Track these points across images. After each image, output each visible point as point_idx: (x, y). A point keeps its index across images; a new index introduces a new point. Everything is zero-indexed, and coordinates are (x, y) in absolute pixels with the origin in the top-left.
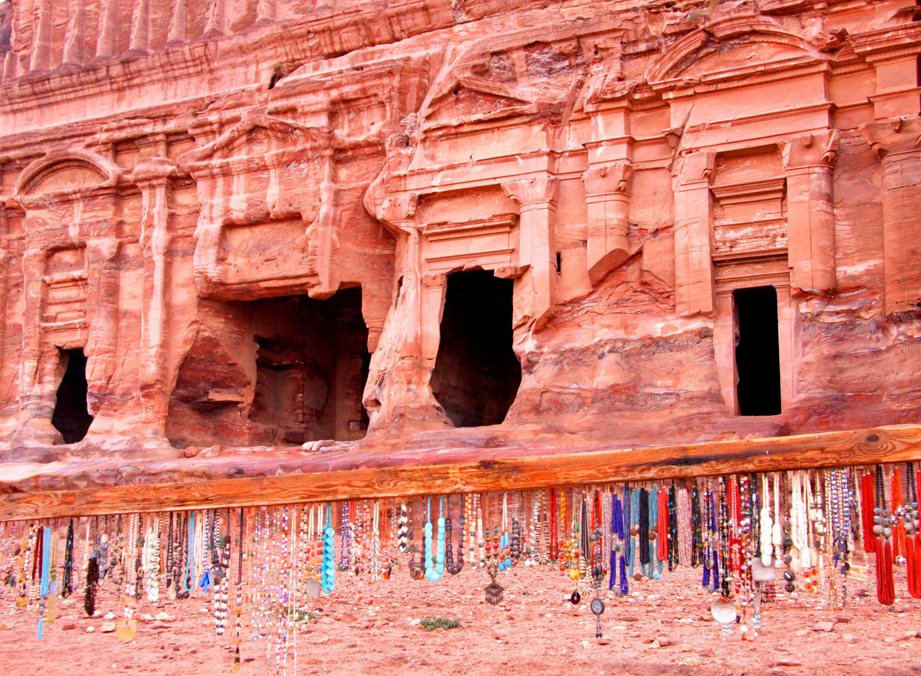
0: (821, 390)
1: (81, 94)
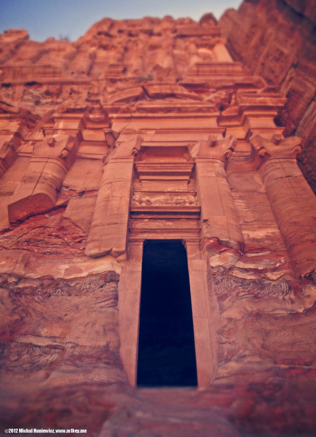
0: (257, 359)
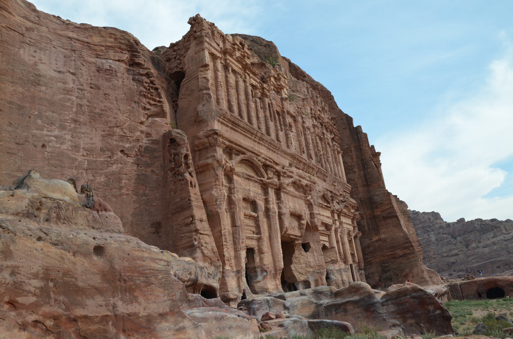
1: (246, 134)
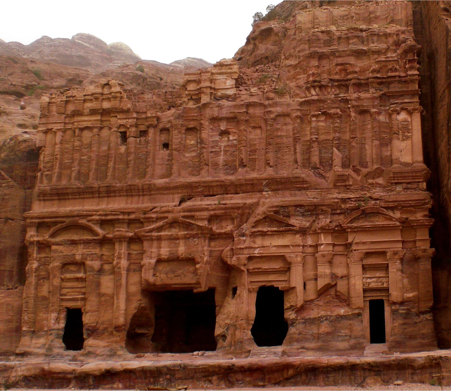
1: (82, 196)
